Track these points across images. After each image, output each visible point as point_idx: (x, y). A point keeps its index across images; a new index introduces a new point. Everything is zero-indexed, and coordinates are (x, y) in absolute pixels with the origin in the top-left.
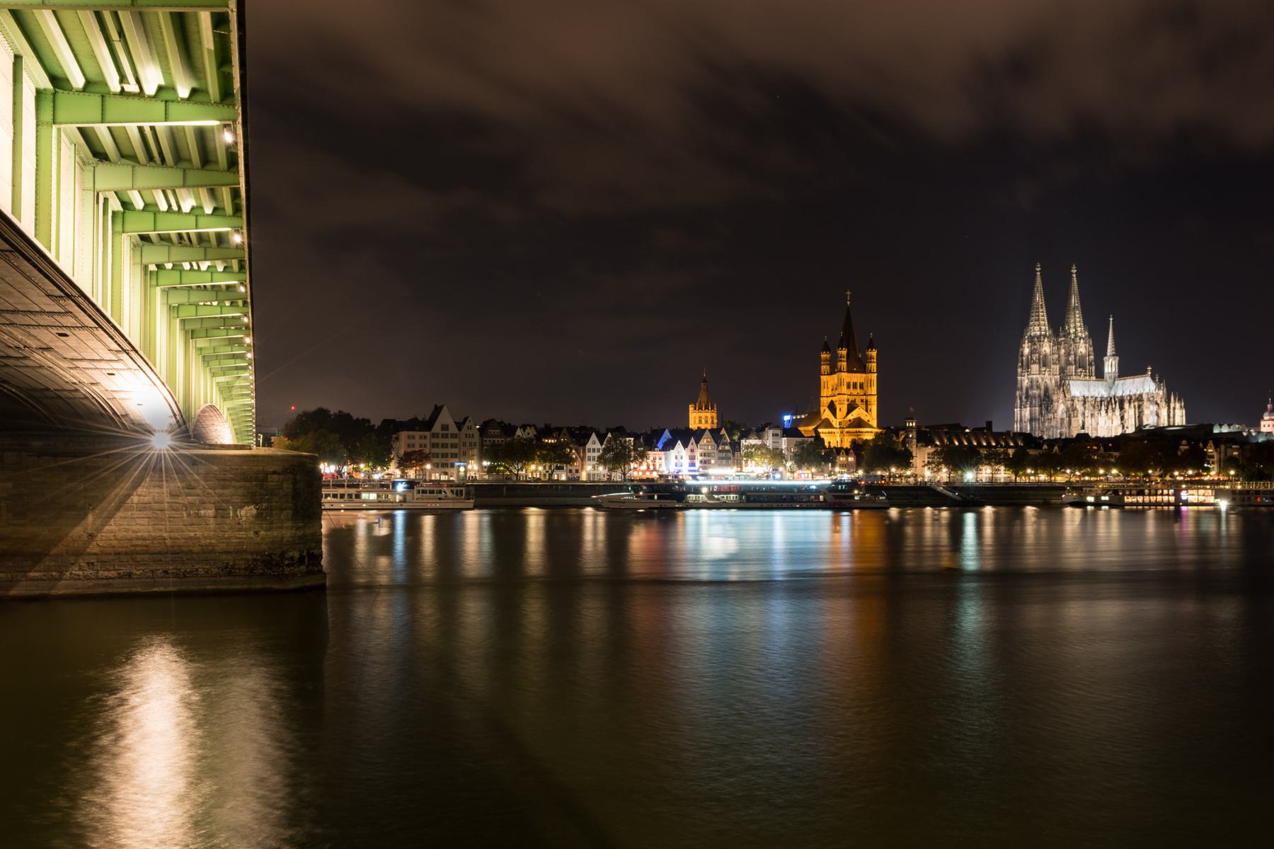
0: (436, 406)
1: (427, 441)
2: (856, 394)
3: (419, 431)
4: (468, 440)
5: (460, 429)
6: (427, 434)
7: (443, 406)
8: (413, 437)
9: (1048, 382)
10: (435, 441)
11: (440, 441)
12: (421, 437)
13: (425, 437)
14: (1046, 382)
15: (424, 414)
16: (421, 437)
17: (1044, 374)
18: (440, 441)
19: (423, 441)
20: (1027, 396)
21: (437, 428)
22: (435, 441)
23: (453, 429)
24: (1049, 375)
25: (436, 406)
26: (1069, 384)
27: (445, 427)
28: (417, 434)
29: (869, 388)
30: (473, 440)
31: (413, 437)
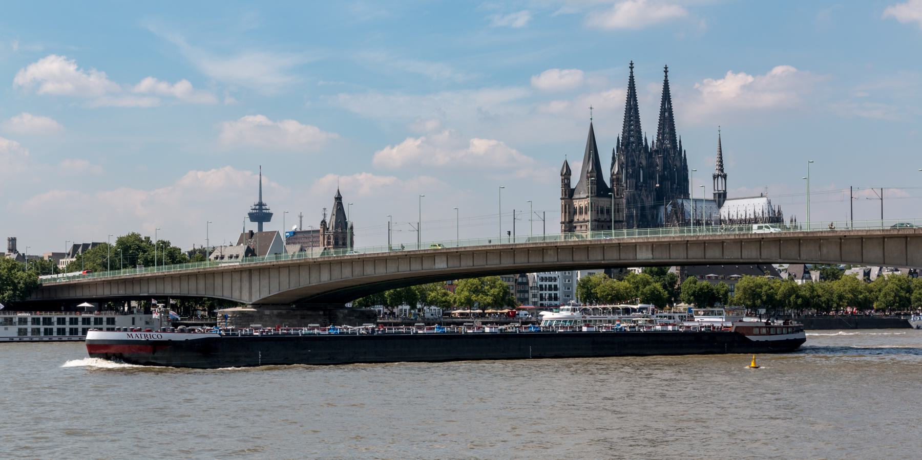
2: (603, 219)
9: (645, 199)
14: (642, 199)
17: (641, 190)
24: (646, 190)
26: (682, 204)
29: (617, 213)
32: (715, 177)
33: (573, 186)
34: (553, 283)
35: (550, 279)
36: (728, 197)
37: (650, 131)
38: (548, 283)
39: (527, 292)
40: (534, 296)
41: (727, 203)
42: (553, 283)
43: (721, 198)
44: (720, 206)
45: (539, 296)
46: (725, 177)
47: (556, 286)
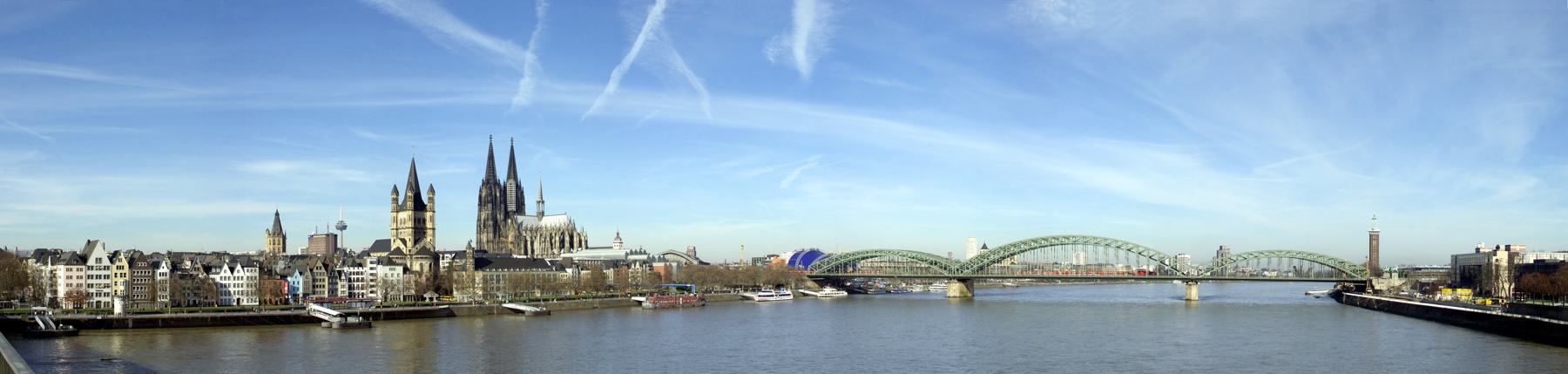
0: (89, 241)
1: (82, 274)
3: (77, 265)
4: (119, 272)
5: (112, 262)
6: (84, 267)
7: (97, 241)
8: (71, 270)
10: (90, 272)
11: (94, 273)
12: (78, 270)
13: (81, 270)
15: (79, 248)
16: (78, 270)
18: (94, 273)
19: (80, 274)
20: (484, 226)
21: (91, 262)
22: (90, 272)
23: (106, 262)
25: (89, 241)
27: (99, 260)
28: (75, 268)
30: (123, 272)
31: (71, 270)
32: (539, 202)
33: (400, 204)
34: (360, 277)
35: (358, 273)
36: (545, 214)
37: (502, 175)
38: (356, 277)
39: (337, 283)
40: (343, 286)
41: (544, 218)
42: (360, 277)
43: (542, 214)
44: (540, 219)
45: (347, 286)
46: (543, 202)
47: (363, 279)
